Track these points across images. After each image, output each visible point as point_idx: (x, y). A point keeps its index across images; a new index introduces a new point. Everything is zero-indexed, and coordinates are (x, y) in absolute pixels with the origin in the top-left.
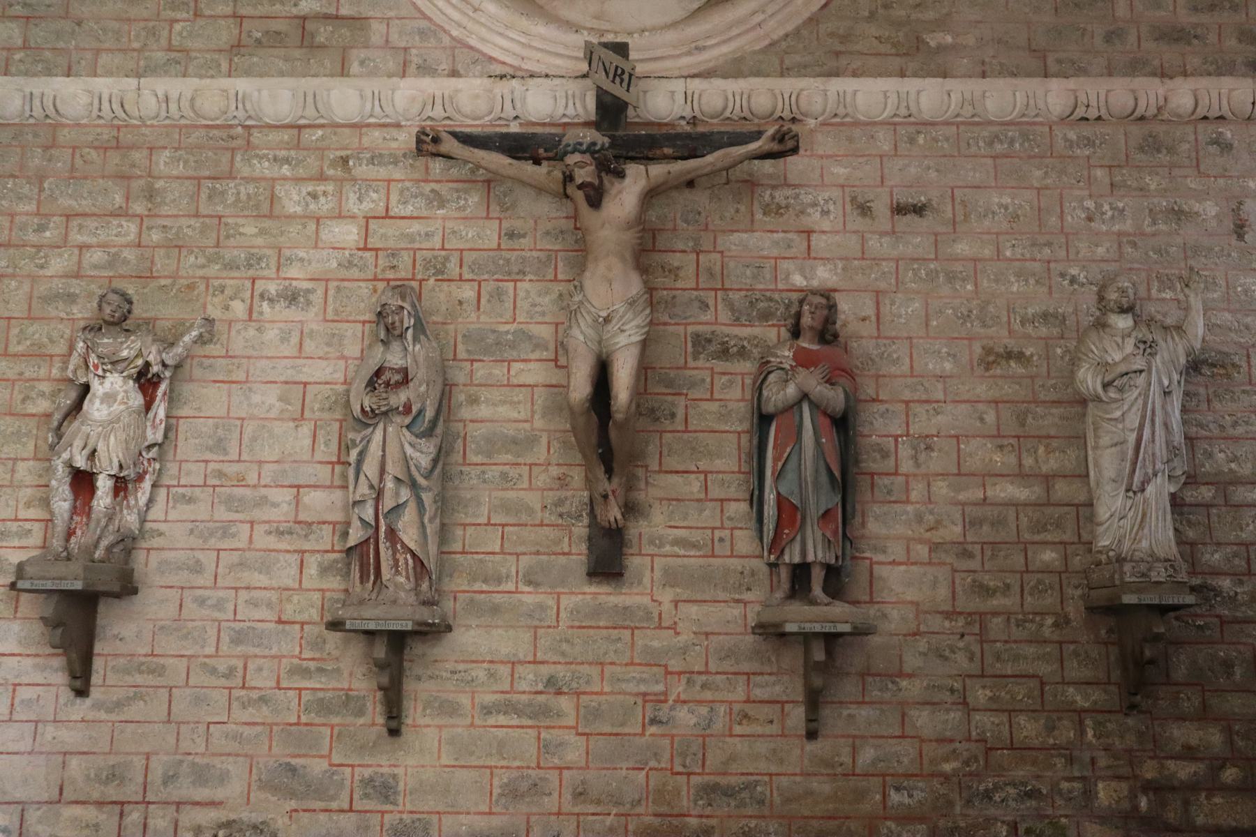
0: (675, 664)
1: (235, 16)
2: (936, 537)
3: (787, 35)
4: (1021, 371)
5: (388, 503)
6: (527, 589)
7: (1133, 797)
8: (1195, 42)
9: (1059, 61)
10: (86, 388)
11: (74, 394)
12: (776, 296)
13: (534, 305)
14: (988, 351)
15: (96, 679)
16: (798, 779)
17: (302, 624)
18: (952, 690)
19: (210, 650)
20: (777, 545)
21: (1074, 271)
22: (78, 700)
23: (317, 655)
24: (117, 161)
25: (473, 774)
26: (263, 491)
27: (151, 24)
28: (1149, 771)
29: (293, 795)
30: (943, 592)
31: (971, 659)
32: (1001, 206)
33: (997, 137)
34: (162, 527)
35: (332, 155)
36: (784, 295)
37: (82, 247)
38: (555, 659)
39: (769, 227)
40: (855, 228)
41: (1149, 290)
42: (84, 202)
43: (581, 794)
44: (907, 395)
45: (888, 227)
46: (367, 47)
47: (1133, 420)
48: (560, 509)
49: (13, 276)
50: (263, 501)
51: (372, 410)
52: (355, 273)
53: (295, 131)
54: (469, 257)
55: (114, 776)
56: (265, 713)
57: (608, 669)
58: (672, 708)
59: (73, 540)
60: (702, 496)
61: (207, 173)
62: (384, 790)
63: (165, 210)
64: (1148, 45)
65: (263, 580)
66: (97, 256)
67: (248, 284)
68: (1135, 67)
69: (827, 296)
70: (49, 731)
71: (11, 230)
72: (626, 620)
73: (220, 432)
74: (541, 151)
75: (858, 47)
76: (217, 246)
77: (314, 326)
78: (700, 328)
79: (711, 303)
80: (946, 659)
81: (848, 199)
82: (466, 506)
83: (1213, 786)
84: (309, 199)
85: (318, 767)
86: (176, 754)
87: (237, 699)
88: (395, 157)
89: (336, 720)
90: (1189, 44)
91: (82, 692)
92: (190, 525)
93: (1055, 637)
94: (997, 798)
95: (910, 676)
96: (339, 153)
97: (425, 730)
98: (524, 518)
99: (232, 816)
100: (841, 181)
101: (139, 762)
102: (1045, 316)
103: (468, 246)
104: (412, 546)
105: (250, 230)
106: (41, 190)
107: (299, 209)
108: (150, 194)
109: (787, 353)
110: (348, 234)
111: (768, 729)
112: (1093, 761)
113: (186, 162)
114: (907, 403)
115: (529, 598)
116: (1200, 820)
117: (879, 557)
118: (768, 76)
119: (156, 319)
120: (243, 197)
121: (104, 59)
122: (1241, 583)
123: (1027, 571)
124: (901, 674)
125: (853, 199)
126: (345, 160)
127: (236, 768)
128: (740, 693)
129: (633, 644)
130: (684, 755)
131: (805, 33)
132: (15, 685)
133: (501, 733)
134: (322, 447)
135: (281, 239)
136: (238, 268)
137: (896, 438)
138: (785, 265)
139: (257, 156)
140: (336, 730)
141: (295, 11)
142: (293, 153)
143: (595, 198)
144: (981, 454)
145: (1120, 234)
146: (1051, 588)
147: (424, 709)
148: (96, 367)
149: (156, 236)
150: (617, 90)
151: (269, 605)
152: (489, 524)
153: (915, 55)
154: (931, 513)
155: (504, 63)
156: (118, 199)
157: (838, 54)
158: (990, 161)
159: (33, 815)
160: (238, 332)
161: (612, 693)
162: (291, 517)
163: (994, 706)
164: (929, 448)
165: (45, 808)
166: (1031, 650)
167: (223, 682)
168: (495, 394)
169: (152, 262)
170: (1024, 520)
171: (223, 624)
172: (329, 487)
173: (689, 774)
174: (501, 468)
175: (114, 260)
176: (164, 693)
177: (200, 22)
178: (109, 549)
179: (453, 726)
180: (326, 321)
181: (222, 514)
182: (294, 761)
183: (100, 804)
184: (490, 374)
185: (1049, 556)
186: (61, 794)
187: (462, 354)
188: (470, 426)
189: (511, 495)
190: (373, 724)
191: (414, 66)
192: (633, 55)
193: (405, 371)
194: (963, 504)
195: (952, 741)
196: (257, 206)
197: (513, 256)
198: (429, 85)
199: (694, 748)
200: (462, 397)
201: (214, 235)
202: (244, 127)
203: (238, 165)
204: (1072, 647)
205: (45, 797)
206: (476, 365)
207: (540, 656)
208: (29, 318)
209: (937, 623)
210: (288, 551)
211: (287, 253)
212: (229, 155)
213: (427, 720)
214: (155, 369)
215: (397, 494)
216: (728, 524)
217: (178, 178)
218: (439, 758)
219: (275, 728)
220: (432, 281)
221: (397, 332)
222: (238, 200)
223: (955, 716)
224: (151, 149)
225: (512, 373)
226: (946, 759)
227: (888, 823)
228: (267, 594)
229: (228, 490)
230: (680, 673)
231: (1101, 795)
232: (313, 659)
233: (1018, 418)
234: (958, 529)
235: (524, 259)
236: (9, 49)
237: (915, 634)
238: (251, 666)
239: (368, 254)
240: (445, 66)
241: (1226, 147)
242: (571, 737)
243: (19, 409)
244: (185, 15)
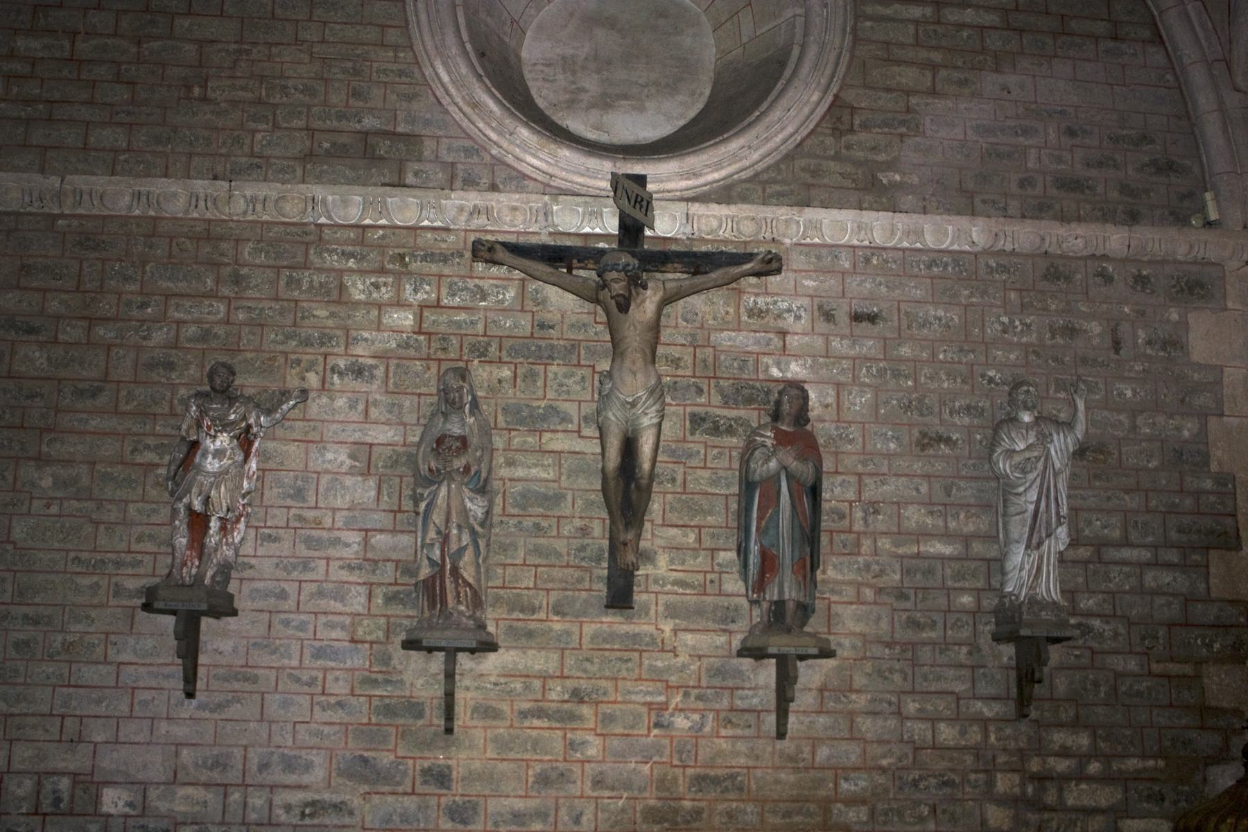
0: (673, 679)
1: (307, 129)
2: (883, 582)
3: (768, 168)
4: (947, 451)
5: (454, 547)
6: (556, 618)
7: (1023, 785)
8: (1087, 191)
9: (984, 202)
10: (195, 445)
11: (185, 449)
12: (758, 384)
13: (561, 385)
14: (924, 435)
15: (200, 685)
16: (770, 771)
17: (372, 643)
18: (890, 703)
19: (295, 663)
20: (760, 586)
21: (991, 373)
22: (186, 701)
23: (384, 669)
24: (208, 249)
25: (512, 765)
26: (337, 533)
27: (236, 133)
28: (1034, 765)
29: (365, 780)
30: (884, 625)
31: (905, 679)
32: (936, 318)
33: (934, 261)
34: (253, 561)
35: (398, 255)
36: (764, 384)
37: (179, 323)
38: (579, 674)
39: (753, 328)
40: (821, 331)
41: (1048, 391)
42: (180, 284)
43: (599, 782)
44: (860, 468)
45: (847, 331)
46: (419, 161)
47: (1033, 495)
48: (583, 554)
49: (121, 346)
50: (337, 542)
51: (438, 470)
52: (412, 352)
53: (360, 230)
54: (507, 343)
55: (220, 764)
56: (337, 716)
57: (620, 683)
58: (672, 715)
59: (185, 570)
60: (697, 546)
61: (285, 263)
62: (441, 777)
63: (249, 293)
64: (1053, 191)
65: (338, 606)
66: (193, 329)
67: (321, 359)
68: (1039, 210)
69: (797, 388)
70: (163, 727)
71: (118, 305)
72: (634, 643)
73: (299, 483)
74: (575, 261)
75: (826, 181)
76: (295, 325)
77: (378, 397)
78: (696, 409)
79: (705, 389)
80: (886, 678)
81: (816, 307)
82: (505, 550)
83: (1080, 776)
84: (372, 288)
85: (386, 759)
86: (269, 746)
87: (318, 703)
88: (445, 256)
89: (401, 721)
90: (1083, 192)
91: (190, 695)
92: (276, 560)
93: (969, 663)
94: (921, 786)
95: (858, 691)
96: (397, 251)
97: (474, 731)
98: (553, 560)
99: (317, 797)
100: (811, 292)
101: (238, 753)
102: (968, 408)
103: (506, 333)
104: (471, 580)
105: (322, 313)
106: (144, 272)
107: (362, 297)
108: (237, 280)
109: (769, 434)
110: (405, 319)
111: (747, 732)
112: (994, 758)
113: (267, 253)
114: (860, 475)
115: (558, 626)
116: (1070, 802)
117: (834, 598)
118: (752, 202)
119: (243, 386)
120: (316, 284)
121: (196, 160)
122: (1108, 622)
123: (949, 611)
124: (851, 690)
125: (820, 307)
126: (402, 257)
127: (318, 759)
128: (725, 703)
129: (640, 666)
130: (680, 752)
131: (783, 166)
132: (134, 688)
133: (534, 733)
134: (386, 498)
135: (350, 322)
136: (312, 345)
137: (851, 503)
138: (765, 359)
139: (327, 250)
140: (400, 729)
141: (358, 127)
142: (358, 249)
143: (624, 307)
144: (914, 516)
145: (1027, 345)
146: (967, 624)
147: (472, 713)
148: (209, 428)
149: (241, 316)
150: (638, 214)
151: (343, 628)
152: (524, 565)
153: (871, 191)
154: (877, 563)
155: (535, 180)
156: (210, 282)
157: (809, 186)
158: (929, 281)
159: (153, 793)
160: (314, 400)
161: (624, 702)
162: (361, 555)
163: (922, 715)
164: (876, 512)
165: (162, 787)
166: (951, 673)
167: (306, 689)
168: (531, 459)
169: (240, 338)
170: (949, 571)
171: (306, 642)
172: (391, 531)
173: (685, 767)
174: (533, 519)
175: (205, 336)
176: (257, 697)
177: (279, 134)
178: (213, 577)
179: (495, 727)
180: (387, 392)
181: (302, 551)
182: (365, 754)
183: (207, 785)
184: (525, 442)
185: (966, 600)
186: (175, 777)
187: (502, 424)
188: (508, 484)
189: (542, 541)
190: (431, 725)
191: (460, 179)
192: (650, 187)
193: (463, 441)
194: (902, 557)
195: (888, 742)
196: (328, 293)
197: (543, 343)
198: (473, 199)
199: (689, 747)
200: (502, 460)
201: (292, 316)
202: (317, 225)
203: (312, 257)
204: (982, 671)
205: (163, 779)
206: (513, 433)
207: (566, 672)
208: (135, 382)
209: (877, 650)
210: (359, 584)
211: (353, 333)
212: (303, 248)
213: (475, 723)
214: (255, 429)
215: (460, 540)
216: (716, 568)
217: (260, 266)
218: (485, 752)
219: (350, 727)
220: (476, 362)
221: (457, 405)
222: (311, 287)
223: (892, 723)
224: (237, 241)
225: (543, 441)
226: (884, 757)
227: (839, 805)
228: (342, 618)
229: (308, 532)
230: (678, 688)
231: (999, 784)
232: (381, 672)
233: (945, 488)
234: (897, 577)
235: (552, 347)
236: (116, 151)
237: (862, 659)
238: (330, 677)
239: (422, 338)
240: (485, 181)
241: (1108, 279)
242: (590, 738)
243: (128, 458)
244: (265, 126)
